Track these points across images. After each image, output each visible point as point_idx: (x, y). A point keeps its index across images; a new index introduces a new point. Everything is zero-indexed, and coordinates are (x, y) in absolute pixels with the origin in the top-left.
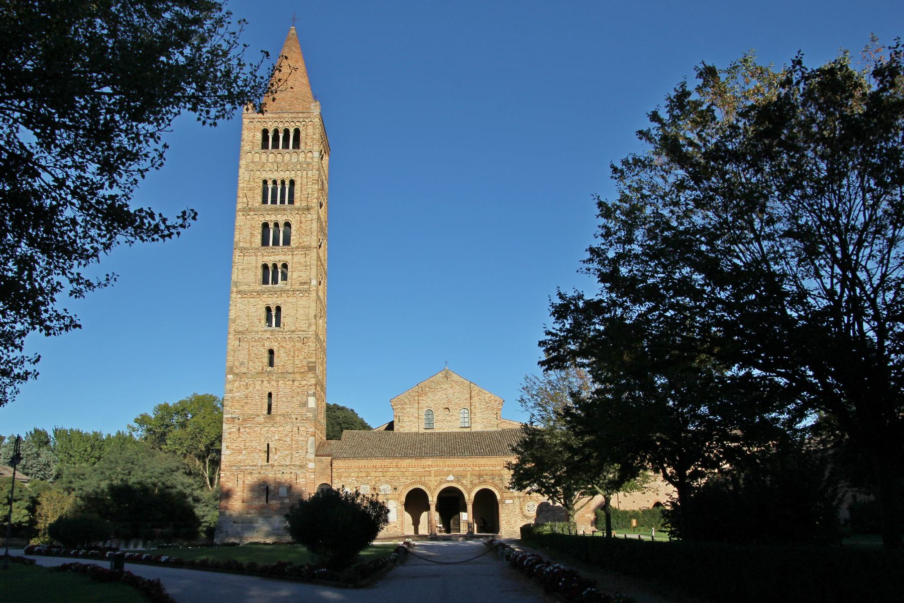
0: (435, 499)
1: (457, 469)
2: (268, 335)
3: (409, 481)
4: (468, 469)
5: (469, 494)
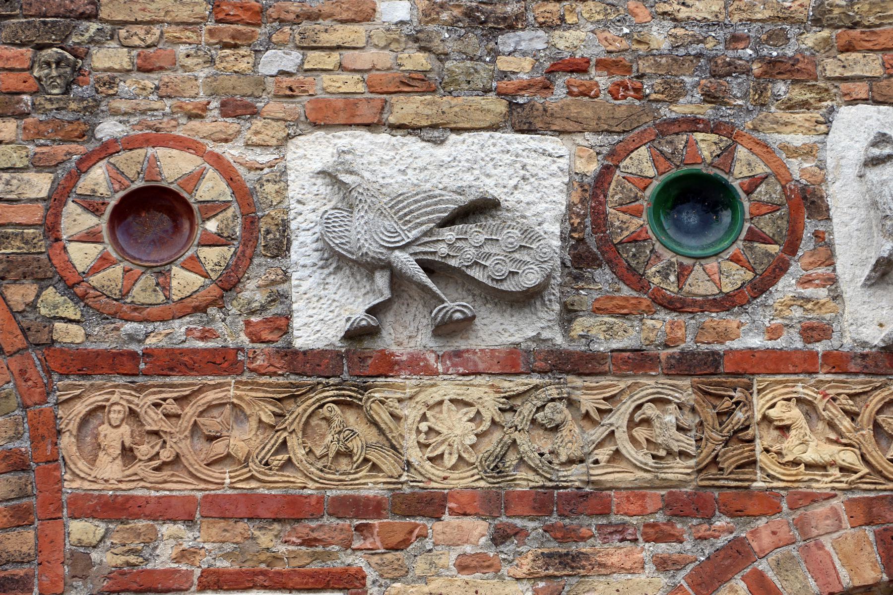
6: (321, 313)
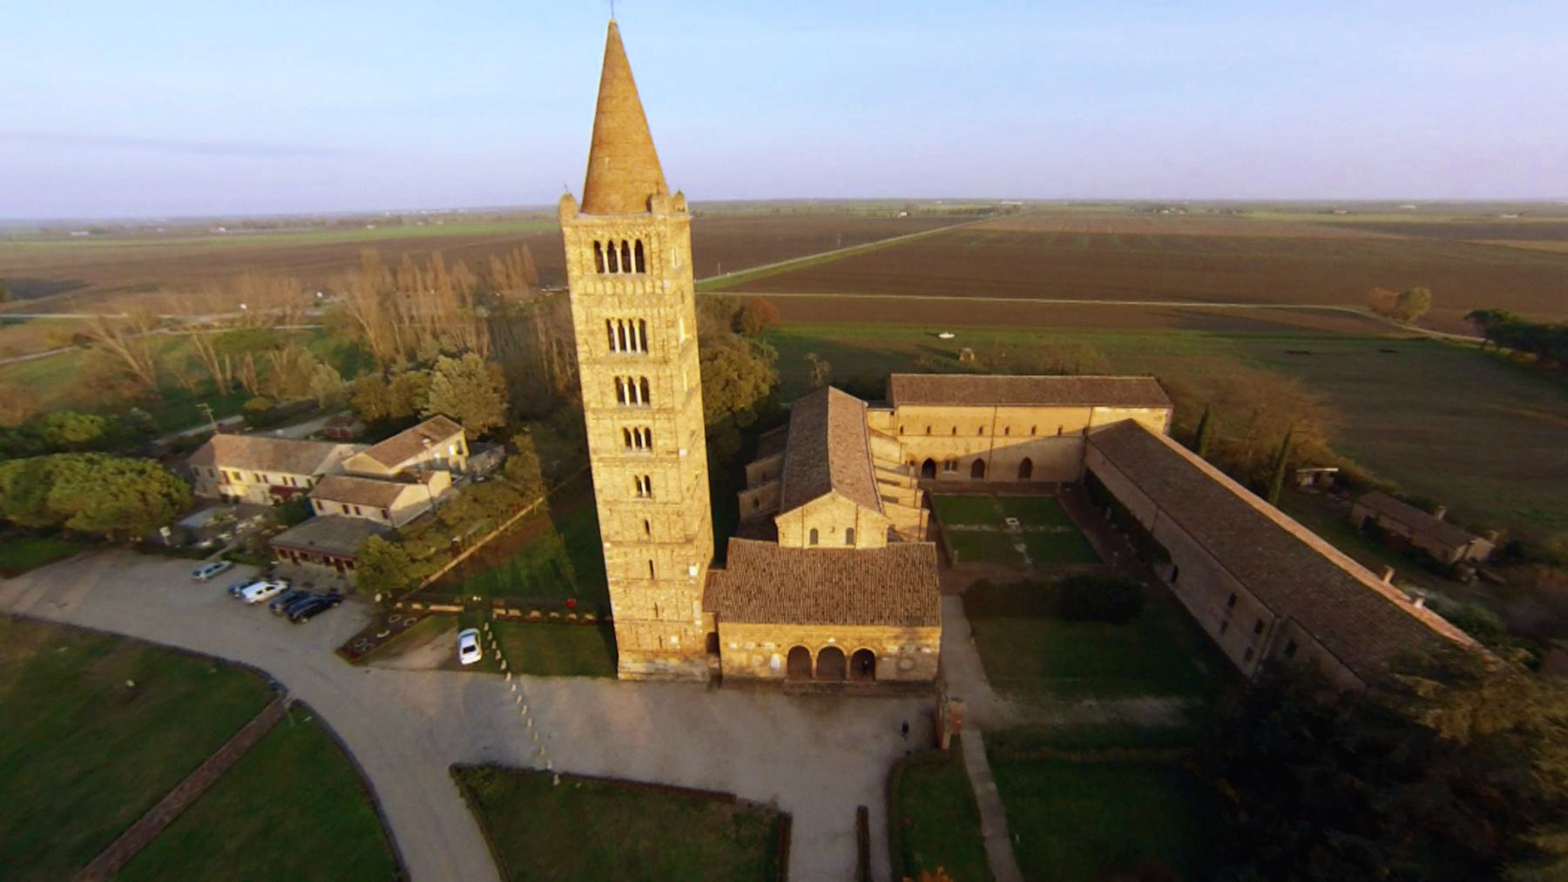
2: (639, 506)
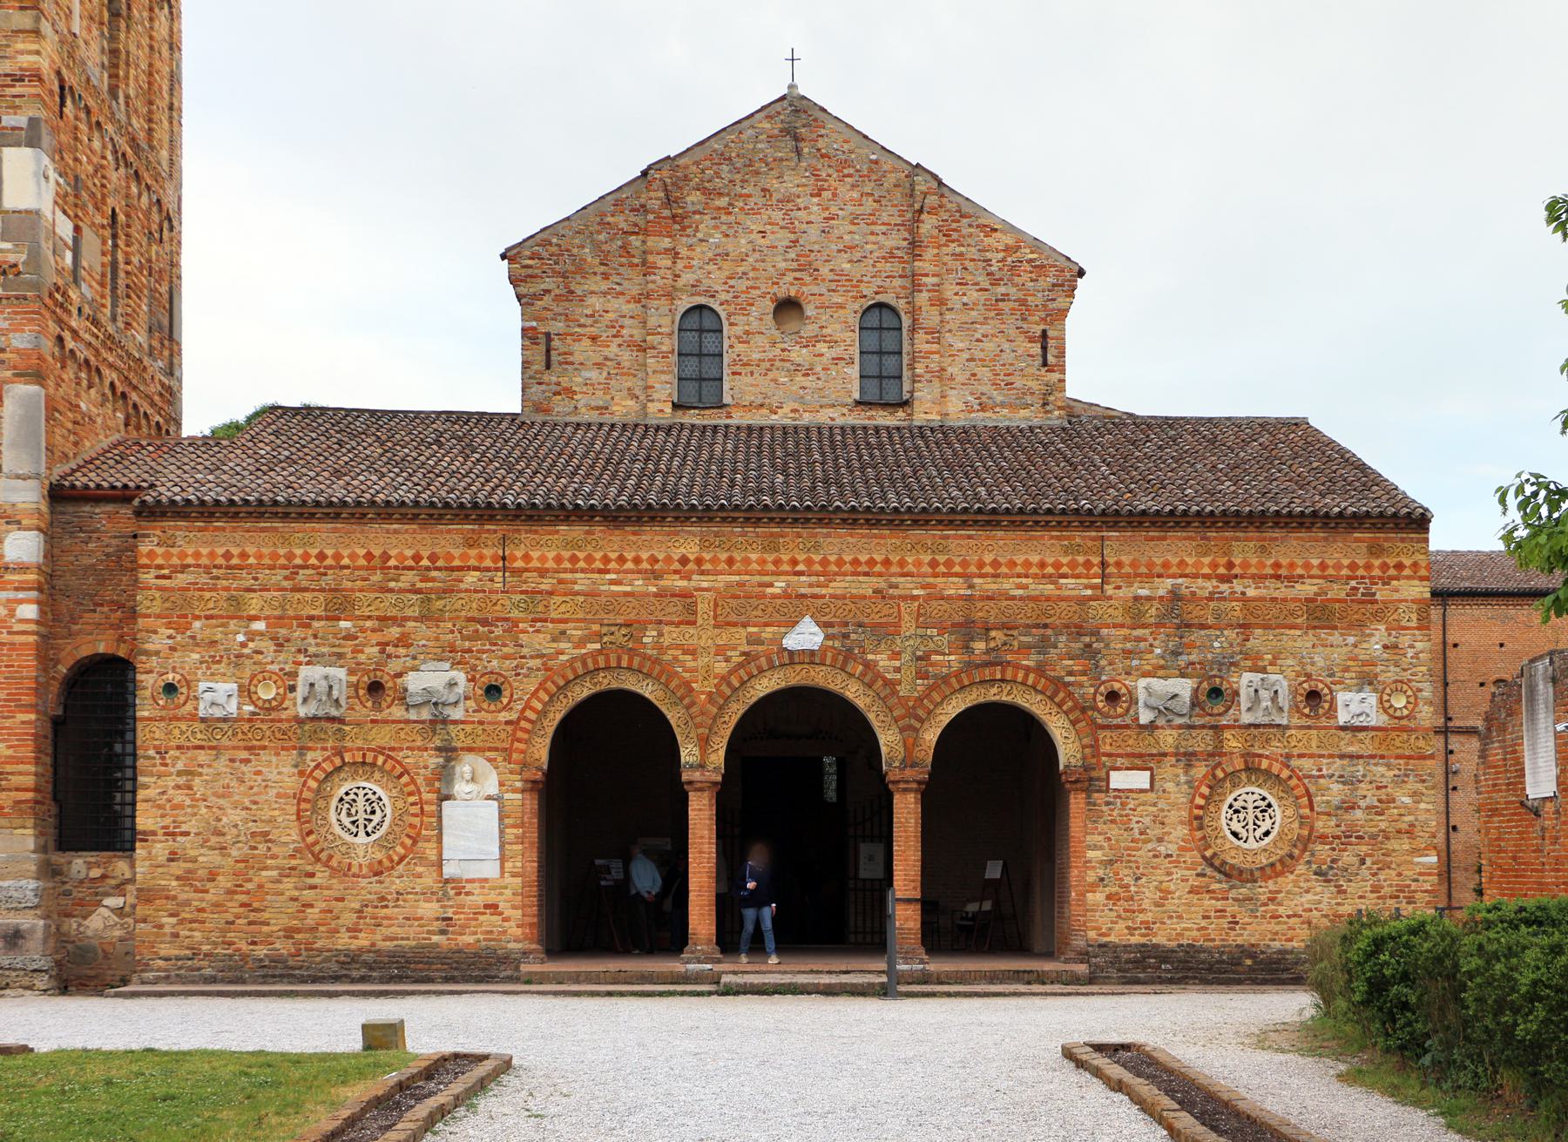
0: (718, 757)
1: (839, 586)
3: (568, 650)
4: (908, 586)
5: (910, 732)
6: (1145, 717)
